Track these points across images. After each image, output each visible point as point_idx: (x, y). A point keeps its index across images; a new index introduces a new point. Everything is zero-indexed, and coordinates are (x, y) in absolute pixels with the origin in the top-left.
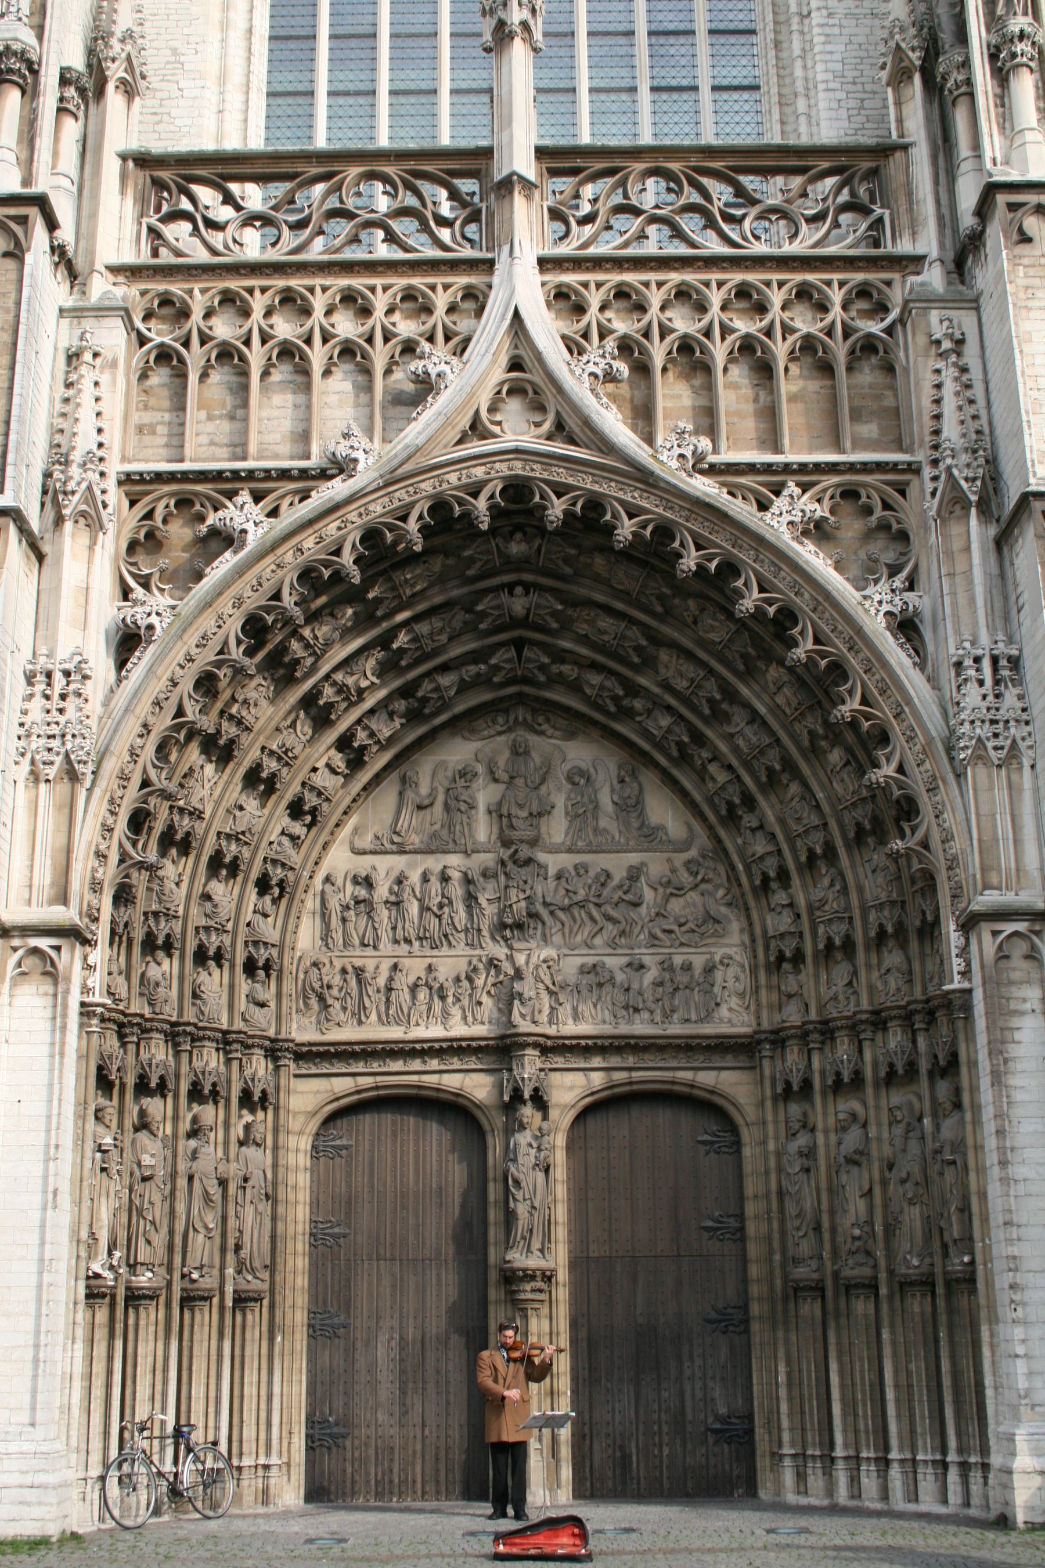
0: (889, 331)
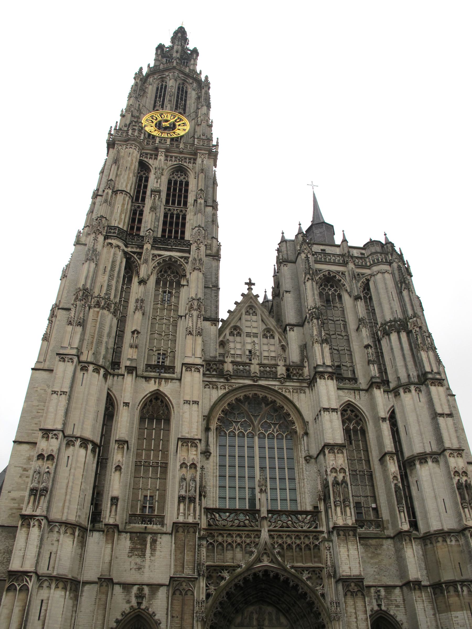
0: (319, 543)
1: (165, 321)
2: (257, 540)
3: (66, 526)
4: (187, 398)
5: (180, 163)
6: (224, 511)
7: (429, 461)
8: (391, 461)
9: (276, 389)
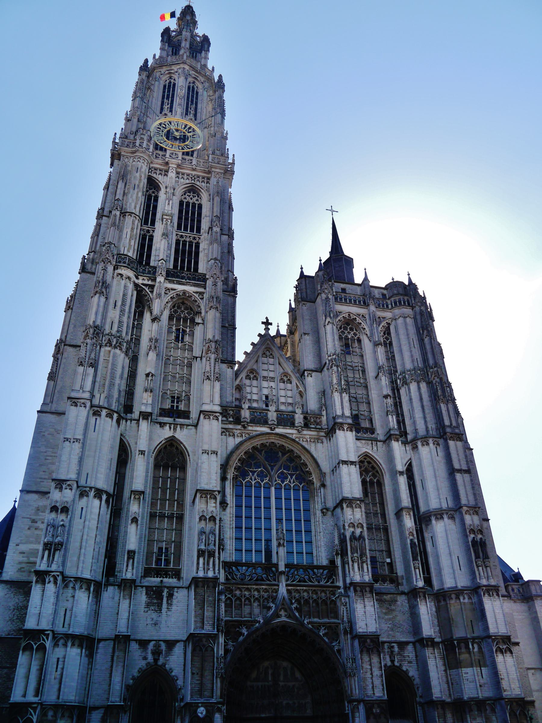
1: (179, 362)
2: (275, 594)
3: (81, 582)
4: (206, 447)
5: (193, 182)
6: (242, 565)
7: (445, 516)
8: (408, 516)
9: (294, 438)
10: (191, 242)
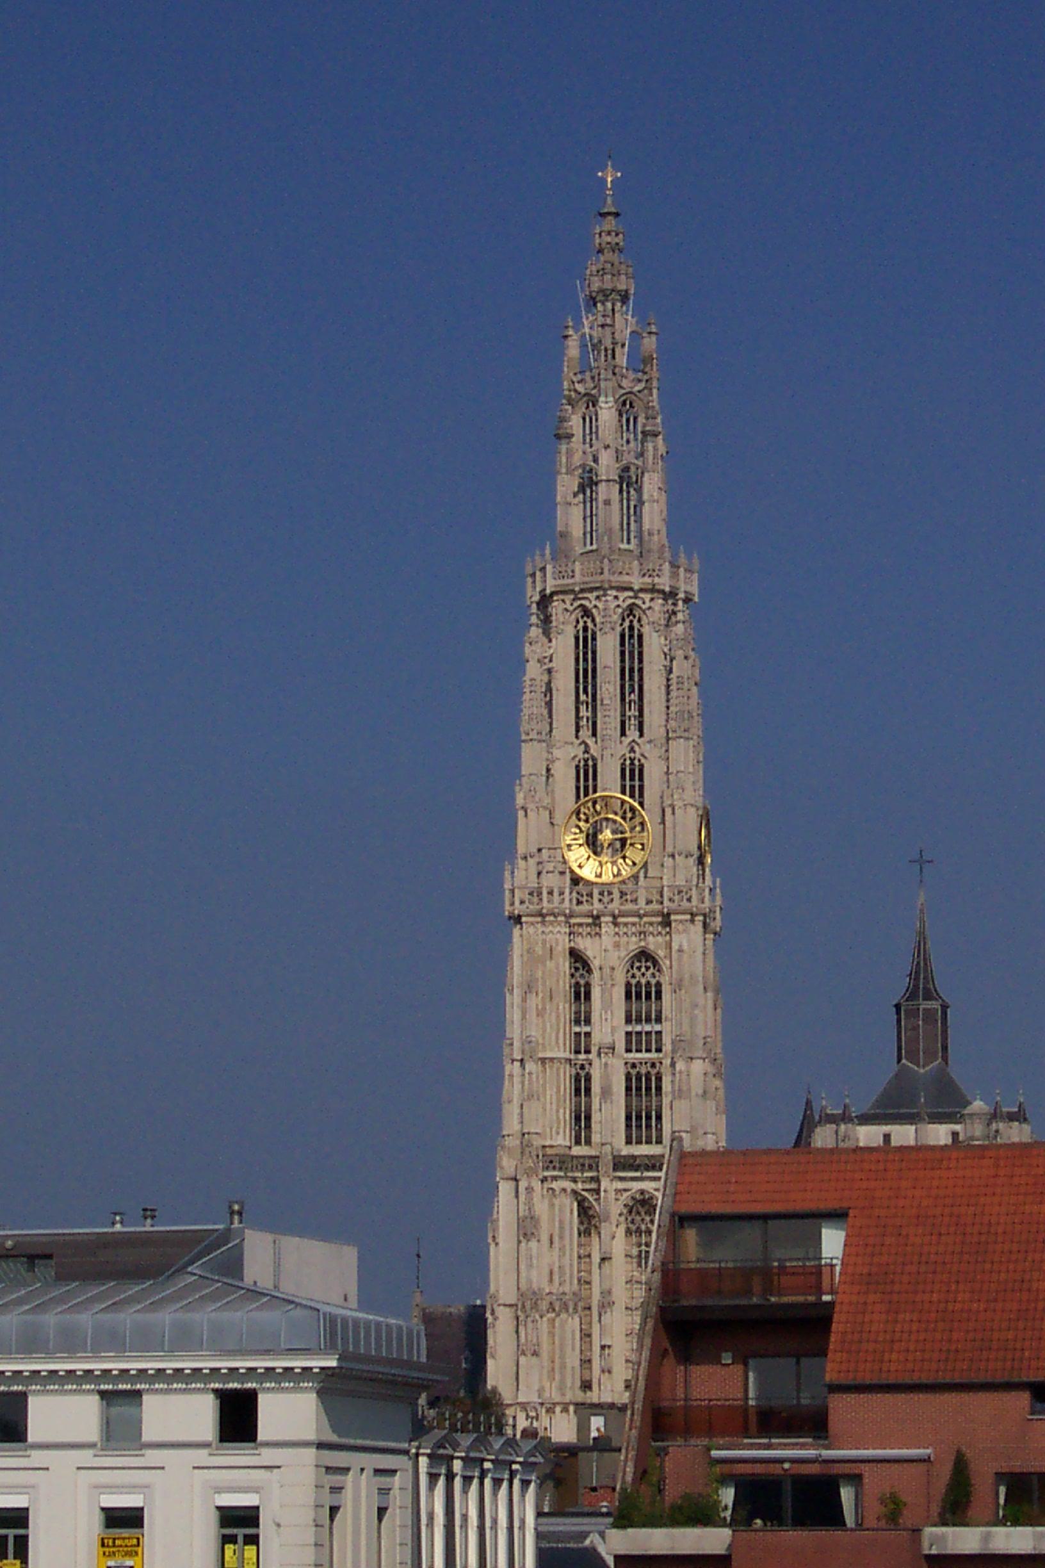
5: (643, 944)
10: (648, 1074)
